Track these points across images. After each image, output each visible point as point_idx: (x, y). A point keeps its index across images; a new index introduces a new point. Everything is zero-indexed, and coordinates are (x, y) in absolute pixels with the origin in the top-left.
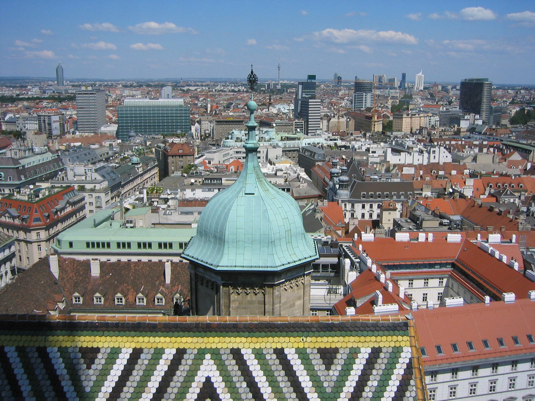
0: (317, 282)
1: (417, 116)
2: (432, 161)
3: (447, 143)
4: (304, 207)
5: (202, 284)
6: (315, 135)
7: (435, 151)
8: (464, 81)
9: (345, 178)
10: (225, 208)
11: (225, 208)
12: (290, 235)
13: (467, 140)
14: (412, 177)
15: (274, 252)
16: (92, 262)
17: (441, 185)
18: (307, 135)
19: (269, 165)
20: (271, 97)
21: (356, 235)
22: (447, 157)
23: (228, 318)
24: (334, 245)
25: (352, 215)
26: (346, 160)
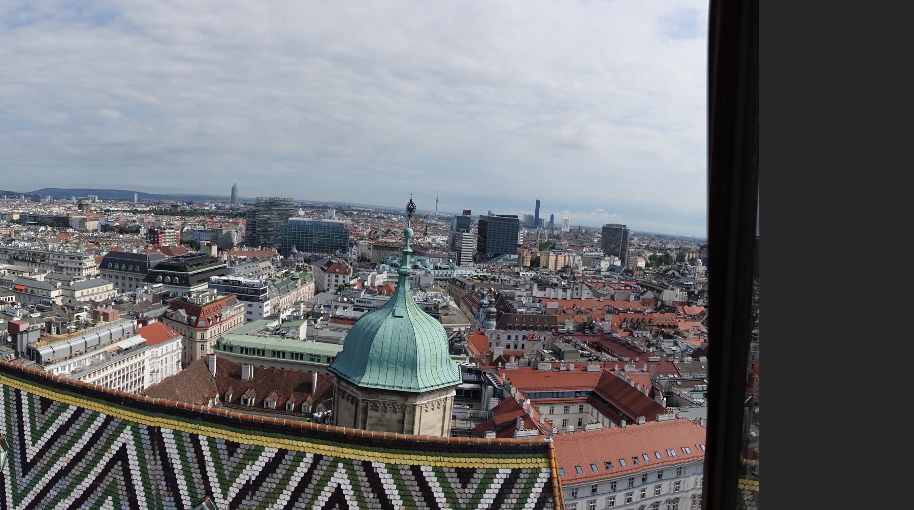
0: (459, 406)
1: (563, 255)
3: (589, 281)
4: (452, 334)
5: (343, 397)
6: (466, 266)
8: (605, 226)
9: (494, 309)
10: (372, 327)
11: (372, 327)
12: (435, 359)
13: (606, 279)
14: (556, 311)
15: (418, 375)
16: (243, 365)
18: (459, 266)
19: (420, 292)
21: (500, 364)
22: (588, 294)
23: (363, 431)
24: (478, 373)
26: (495, 293)
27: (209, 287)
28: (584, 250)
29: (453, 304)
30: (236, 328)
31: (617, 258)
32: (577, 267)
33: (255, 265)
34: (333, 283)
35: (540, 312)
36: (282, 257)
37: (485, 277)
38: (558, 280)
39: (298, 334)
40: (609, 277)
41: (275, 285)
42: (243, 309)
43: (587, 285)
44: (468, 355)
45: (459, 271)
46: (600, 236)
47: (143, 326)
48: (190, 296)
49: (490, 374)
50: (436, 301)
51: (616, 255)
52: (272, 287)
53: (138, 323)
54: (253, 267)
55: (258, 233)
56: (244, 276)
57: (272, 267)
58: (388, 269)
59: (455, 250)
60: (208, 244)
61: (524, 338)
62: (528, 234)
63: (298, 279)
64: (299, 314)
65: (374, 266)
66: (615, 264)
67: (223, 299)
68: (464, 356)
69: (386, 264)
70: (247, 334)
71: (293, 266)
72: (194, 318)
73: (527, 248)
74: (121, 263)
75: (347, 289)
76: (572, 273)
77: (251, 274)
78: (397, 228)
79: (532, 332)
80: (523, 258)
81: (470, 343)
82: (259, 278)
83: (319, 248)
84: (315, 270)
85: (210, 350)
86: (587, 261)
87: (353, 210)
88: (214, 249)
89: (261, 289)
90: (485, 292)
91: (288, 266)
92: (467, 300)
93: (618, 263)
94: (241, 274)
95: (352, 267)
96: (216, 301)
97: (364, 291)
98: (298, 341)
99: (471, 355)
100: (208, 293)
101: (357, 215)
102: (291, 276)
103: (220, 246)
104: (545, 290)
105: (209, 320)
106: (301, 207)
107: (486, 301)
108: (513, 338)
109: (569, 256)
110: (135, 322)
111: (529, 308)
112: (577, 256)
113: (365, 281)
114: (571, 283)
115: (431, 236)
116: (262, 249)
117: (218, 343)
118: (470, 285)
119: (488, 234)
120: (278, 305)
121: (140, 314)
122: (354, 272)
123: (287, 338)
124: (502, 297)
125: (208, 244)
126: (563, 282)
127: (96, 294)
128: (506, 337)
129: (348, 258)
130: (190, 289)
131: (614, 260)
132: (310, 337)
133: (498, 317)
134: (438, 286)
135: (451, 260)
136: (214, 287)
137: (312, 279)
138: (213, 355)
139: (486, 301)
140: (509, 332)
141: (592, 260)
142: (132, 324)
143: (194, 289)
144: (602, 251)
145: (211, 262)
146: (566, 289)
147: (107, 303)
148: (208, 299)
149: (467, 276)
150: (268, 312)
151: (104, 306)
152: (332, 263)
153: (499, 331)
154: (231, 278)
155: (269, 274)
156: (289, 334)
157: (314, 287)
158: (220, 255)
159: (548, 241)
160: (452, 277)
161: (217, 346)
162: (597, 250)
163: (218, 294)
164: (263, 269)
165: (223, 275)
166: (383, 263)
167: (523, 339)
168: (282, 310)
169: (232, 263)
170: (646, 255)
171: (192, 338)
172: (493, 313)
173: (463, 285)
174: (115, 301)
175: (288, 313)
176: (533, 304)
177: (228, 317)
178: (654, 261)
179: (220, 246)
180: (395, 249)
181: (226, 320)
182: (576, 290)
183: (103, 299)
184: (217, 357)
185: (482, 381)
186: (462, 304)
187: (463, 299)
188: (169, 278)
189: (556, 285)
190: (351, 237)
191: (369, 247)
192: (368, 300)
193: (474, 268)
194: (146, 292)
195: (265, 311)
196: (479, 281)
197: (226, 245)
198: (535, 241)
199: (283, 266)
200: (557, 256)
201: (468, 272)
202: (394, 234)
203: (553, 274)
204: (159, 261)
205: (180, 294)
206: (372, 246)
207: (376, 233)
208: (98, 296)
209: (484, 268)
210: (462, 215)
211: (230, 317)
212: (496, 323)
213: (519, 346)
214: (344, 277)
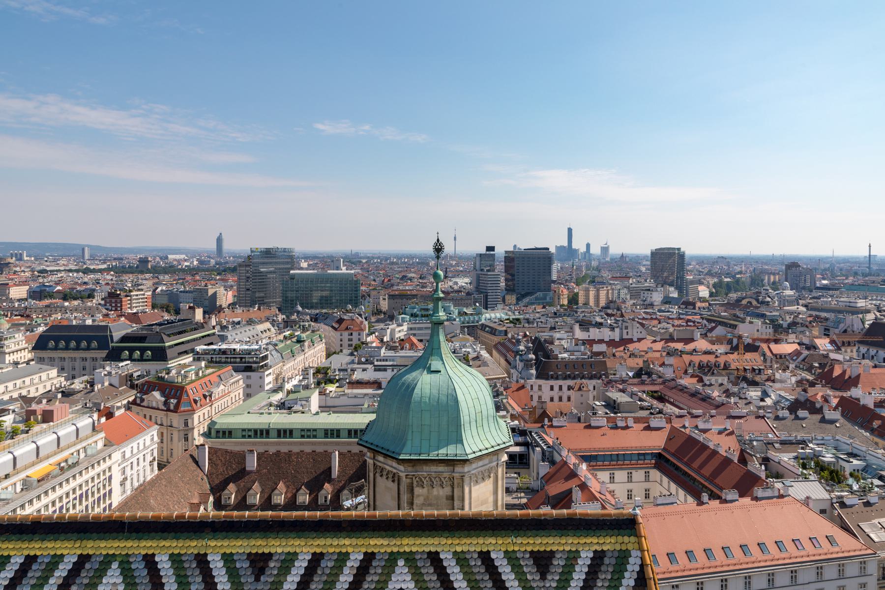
1: (605, 289)
2: (625, 336)
7: (627, 327)
17: (637, 364)
20: (448, 270)
21: (546, 420)
22: (641, 332)
24: (523, 433)
25: (540, 397)
26: (531, 337)
27: (194, 359)
28: (631, 281)
29: (484, 354)
30: (234, 407)
31: (672, 289)
32: (624, 302)
33: (251, 328)
34: (346, 343)
35: (586, 357)
36: (284, 316)
37: (518, 320)
38: (602, 318)
39: (310, 406)
40: (664, 312)
41: (276, 350)
42: (241, 382)
43: (638, 322)
44: (508, 412)
45: (488, 316)
46: (649, 263)
47: (107, 419)
48: (168, 373)
49: (536, 433)
50: (465, 351)
51: (671, 285)
52: (274, 352)
53: (100, 417)
54: (249, 330)
55: (253, 290)
56: (240, 341)
57: (272, 329)
58: (408, 320)
59: (482, 293)
60: (190, 308)
61: (570, 388)
62: (561, 268)
63: (304, 341)
64: (308, 382)
65: (392, 318)
66: (671, 295)
67: (213, 373)
68: (504, 413)
69: (405, 314)
70: (249, 413)
71: (298, 326)
72: (173, 401)
73: (563, 284)
74: (68, 340)
75: (364, 349)
76: (618, 309)
77: (248, 340)
78: (413, 273)
79: (579, 381)
80: (559, 296)
81: (509, 398)
82: (257, 343)
83: (325, 302)
84: (325, 330)
85: (199, 440)
86: (635, 293)
87: (361, 258)
88: (199, 315)
89: (261, 356)
90: (520, 337)
91: (292, 327)
92: (500, 347)
93: (675, 295)
94: (236, 340)
95: (367, 323)
96: (204, 376)
97: (384, 348)
98: (309, 415)
99: (511, 411)
100: (193, 367)
101: (366, 262)
102: (296, 338)
103: (205, 309)
104: (588, 331)
105: (195, 401)
106: (302, 258)
107: (522, 348)
108: (556, 388)
109: (613, 289)
110: (95, 416)
111: (572, 352)
112: (623, 289)
113: (384, 336)
114: (619, 321)
115: (452, 279)
116: (259, 309)
117: (210, 429)
118: (502, 331)
120: (281, 373)
121: (103, 404)
122: (369, 328)
123: (295, 412)
124: (540, 341)
125: (190, 308)
126: (609, 322)
127: (28, 386)
128: (549, 388)
129: (362, 313)
130: (168, 364)
131: (669, 291)
132: (324, 408)
133: (538, 364)
134: (466, 334)
135: (477, 304)
136: (199, 359)
137: (321, 340)
138: (203, 445)
139: (522, 348)
140: (552, 382)
141: (642, 292)
142: (90, 420)
143: (172, 364)
144: (652, 281)
145: (195, 329)
146: (614, 328)
147: (49, 396)
148: (193, 375)
149: (497, 321)
150: (270, 383)
151: (44, 401)
152: (344, 320)
153: (541, 382)
154: (224, 346)
155: (269, 338)
156: (296, 408)
157: (325, 349)
158: (207, 319)
160: (480, 323)
161: (207, 435)
162: (646, 281)
163: (207, 367)
164: (261, 332)
165: (212, 344)
166: (402, 314)
167: (569, 389)
168: (286, 380)
169: (224, 328)
170: (708, 282)
171: (172, 427)
172: (531, 360)
173: (493, 332)
174: (63, 392)
175: (295, 382)
176: (577, 348)
177: (221, 395)
178: (718, 289)
179: (205, 309)
180: (415, 296)
181: (219, 398)
182: (625, 329)
183: (42, 391)
184: (209, 448)
185: (528, 442)
186: (494, 352)
187: (495, 346)
188: (138, 352)
189: (601, 324)
190: (363, 288)
191: (384, 297)
192: (390, 358)
194: (109, 374)
195: (266, 382)
196: (512, 325)
197: (212, 307)
198: (570, 275)
199: (286, 327)
200: (598, 291)
201: (498, 315)
202: (411, 280)
203: (596, 311)
204: (123, 333)
205: (153, 372)
206: (387, 295)
207: (389, 280)
208: (33, 389)
211: (225, 395)
212: (535, 372)
213: (565, 398)
214: (359, 335)
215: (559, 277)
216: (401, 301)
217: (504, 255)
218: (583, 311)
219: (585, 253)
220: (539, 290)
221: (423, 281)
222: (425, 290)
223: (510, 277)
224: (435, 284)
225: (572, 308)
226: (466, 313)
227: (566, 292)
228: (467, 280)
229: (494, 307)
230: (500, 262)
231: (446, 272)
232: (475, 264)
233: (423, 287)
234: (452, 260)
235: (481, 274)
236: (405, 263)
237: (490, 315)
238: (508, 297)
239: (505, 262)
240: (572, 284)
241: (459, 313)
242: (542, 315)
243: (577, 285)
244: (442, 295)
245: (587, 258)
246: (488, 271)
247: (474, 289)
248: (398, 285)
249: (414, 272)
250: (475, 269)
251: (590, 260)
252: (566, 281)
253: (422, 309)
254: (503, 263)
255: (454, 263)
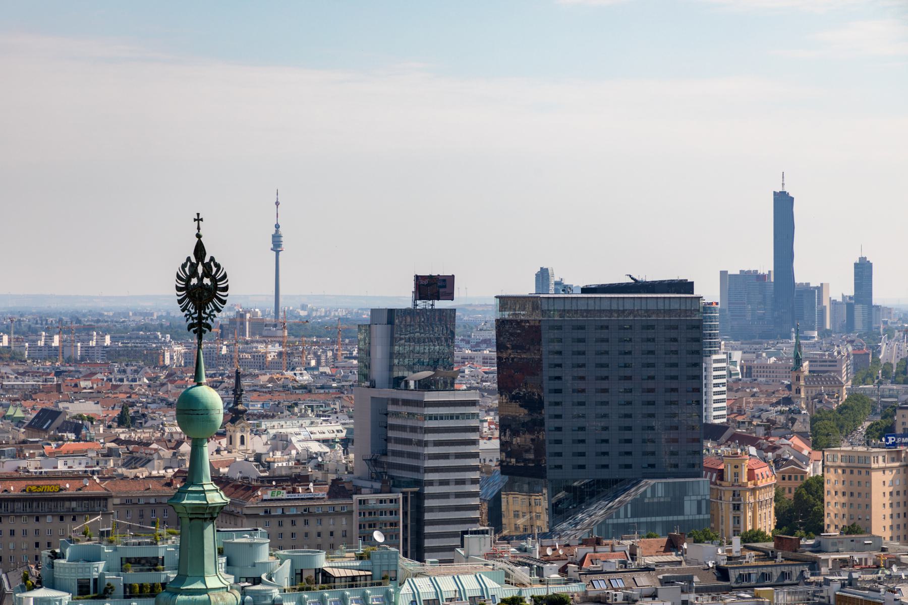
20: (245, 383)
59: (395, 484)
62: (748, 371)
69: (52, 586)
73: (753, 441)
78: (88, 397)
115: (265, 424)
119: (548, 385)
135: (378, 536)
159: (854, 396)
166: (39, 583)
193: (499, 565)
198: (787, 401)
201: (470, 584)
209: (547, 560)
210: (409, 304)
215: (735, 410)
216: (32, 525)
217: (493, 315)
218: (844, 563)
219: (849, 305)
220: (652, 471)
221: (135, 436)
222: (142, 473)
223: (520, 412)
224: (186, 448)
225: (795, 546)
226: (326, 578)
227: (767, 477)
228: (333, 429)
229: (452, 549)
230: (476, 347)
231: (237, 392)
232: (366, 355)
233: (133, 461)
234: (267, 339)
235: (395, 402)
236: (52, 353)
237: (435, 585)
238: (512, 503)
239: (500, 347)
240: (796, 441)
241: (297, 576)
242: (666, 582)
243: (816, 446)
244: (216, 498)
245: (859, 325)
246: (425, 385)
247: (363, 469)
248: (19, 455)
249: (94, 396)
250: (365, 376)
251: (872, 336)
252: (770, 426)
253: (128, 562)
254: (489, 352)
255: (272, 351)
